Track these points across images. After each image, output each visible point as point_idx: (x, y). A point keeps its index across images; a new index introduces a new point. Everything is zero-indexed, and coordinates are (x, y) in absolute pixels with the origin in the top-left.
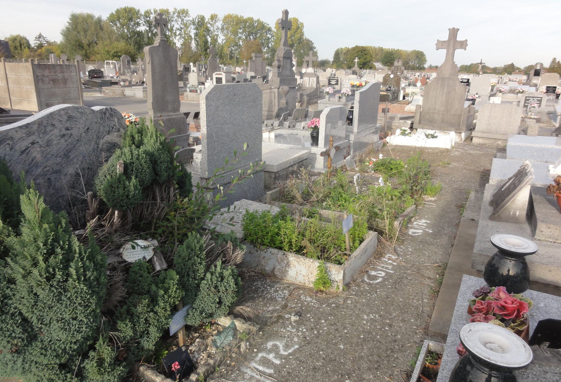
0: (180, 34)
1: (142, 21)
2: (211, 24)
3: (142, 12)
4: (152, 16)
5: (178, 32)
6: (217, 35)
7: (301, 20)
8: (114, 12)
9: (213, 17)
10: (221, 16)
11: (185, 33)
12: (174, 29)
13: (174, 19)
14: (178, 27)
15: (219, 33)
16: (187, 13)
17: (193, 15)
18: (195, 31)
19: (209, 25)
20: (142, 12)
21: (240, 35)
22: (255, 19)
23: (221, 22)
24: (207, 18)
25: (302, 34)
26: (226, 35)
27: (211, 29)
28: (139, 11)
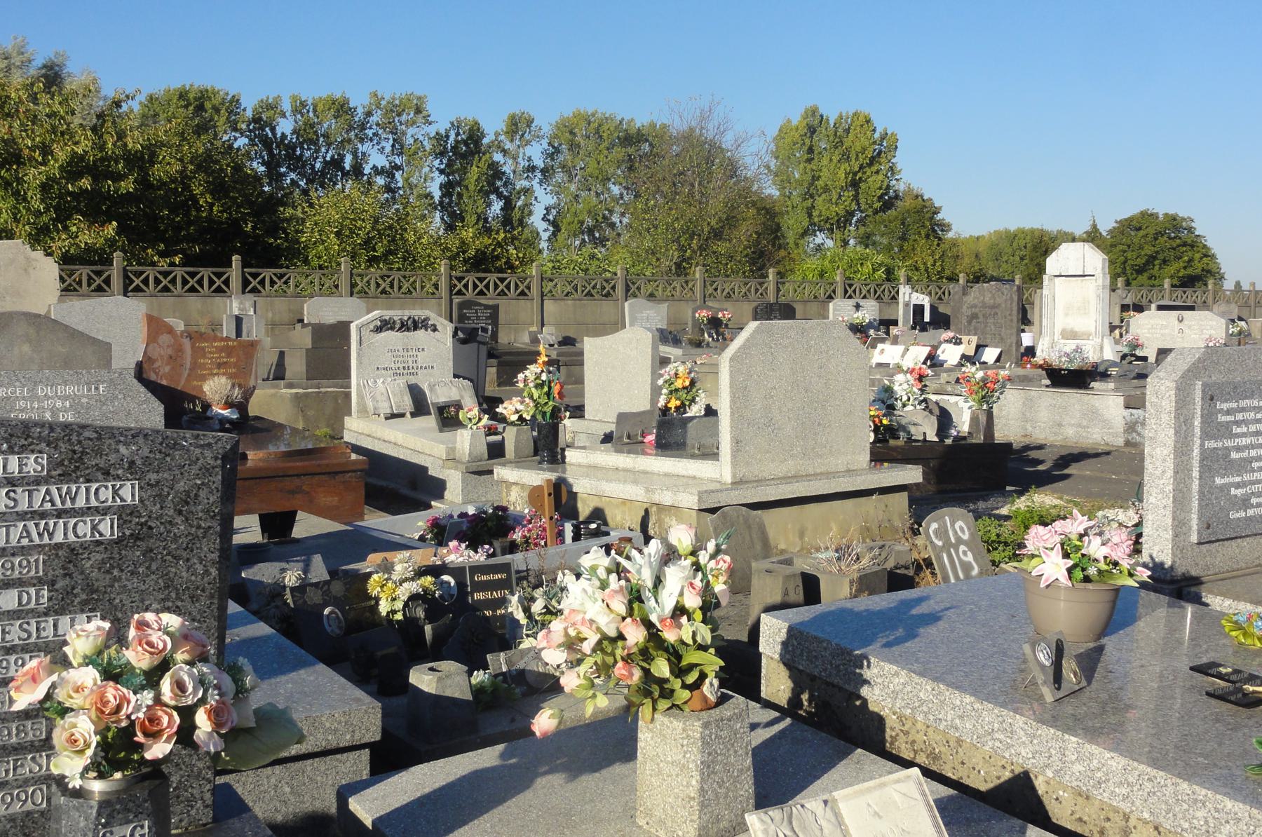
2: (505, 152)
3: (249, 106)
4: (285, 127)
6: (527, 191)
7: (881, 124)
8: (135, 106)
9: (518, 126)
10: (546, 121)
12: (367, 170)
13: (370, 133)
15: (535, 182)
17: (443, 116)
19: (498, 157)
20: (249, 106)
23: (545, 142)
24: (492, 127)
27: (508, 169)
28: (236, 101)
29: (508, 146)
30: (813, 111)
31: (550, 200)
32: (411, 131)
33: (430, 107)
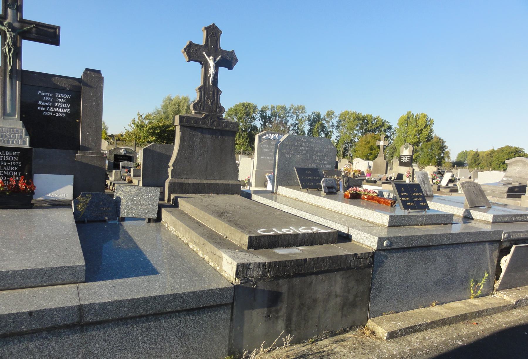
0: (293, 129)
1: (258, 116)
2: (326, 121)
4: (269, 113)
5: (292, 128)
7: (429, 117)
9: (330, 114)
10: (338, 113)
11: (298, 129)
13: (290, 115)
14: (293, 122)
16: (303, 109)
17: (309, 112)
18: (309, 127)
19: (324, 122)
20: (260, 108)
21: (356, 132)
22: (375, 116)
23: (337, 119)
24: (323, 114)
25: (431, 130)
26: (340, 132)
27: (326, 126)
29: (327, 119)
30: (410, 113)
31: (338, 134)
32: (301, 115)
33: (306, 109)
